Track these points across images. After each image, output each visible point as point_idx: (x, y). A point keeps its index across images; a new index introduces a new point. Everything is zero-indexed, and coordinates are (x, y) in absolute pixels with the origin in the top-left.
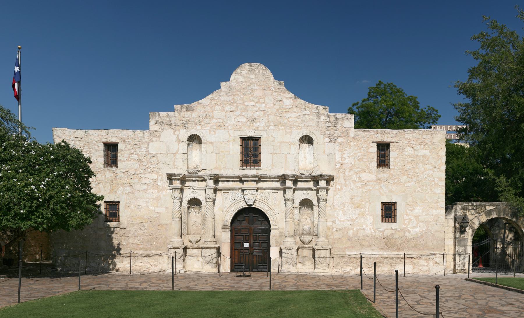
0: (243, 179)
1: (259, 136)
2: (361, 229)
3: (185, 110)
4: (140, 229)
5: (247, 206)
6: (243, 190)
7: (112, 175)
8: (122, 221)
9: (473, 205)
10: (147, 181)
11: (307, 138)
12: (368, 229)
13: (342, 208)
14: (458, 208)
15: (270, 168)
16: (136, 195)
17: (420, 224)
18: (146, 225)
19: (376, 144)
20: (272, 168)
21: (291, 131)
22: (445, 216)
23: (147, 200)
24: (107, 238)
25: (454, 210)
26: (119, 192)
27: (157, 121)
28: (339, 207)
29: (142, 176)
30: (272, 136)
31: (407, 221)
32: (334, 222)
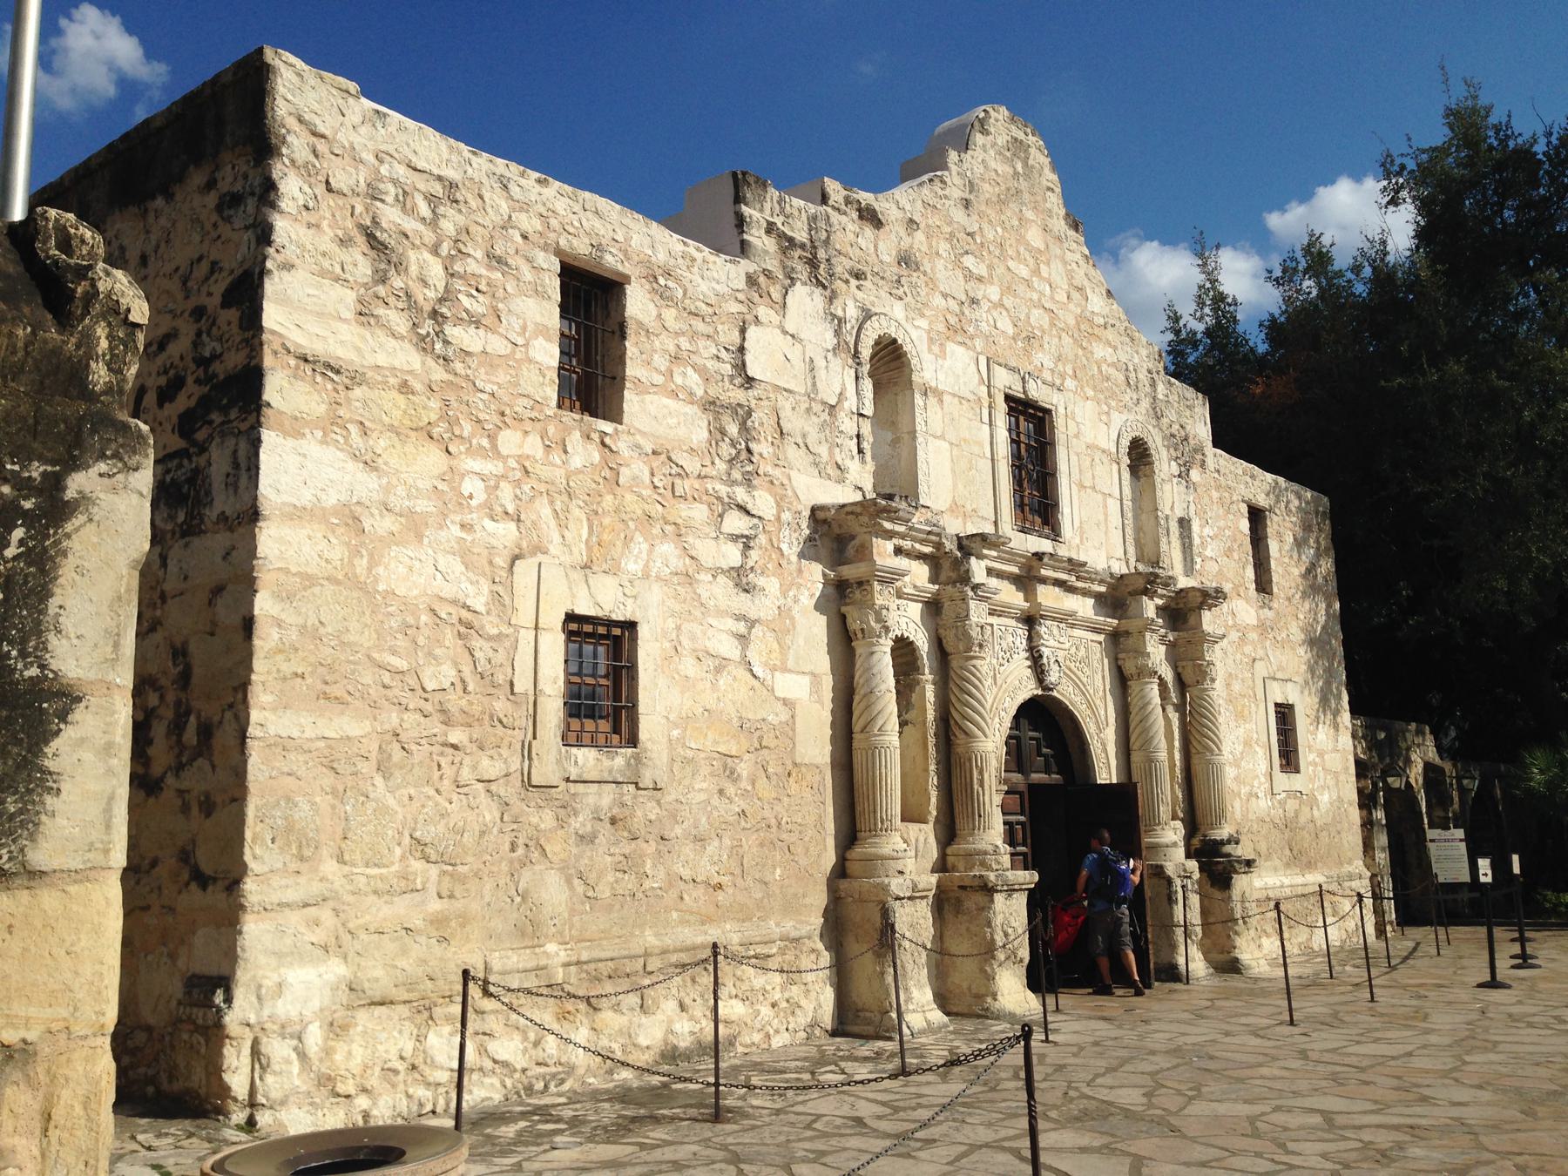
0: (1043, 572)
1: (1048, 406)
3: (855, 215)
4: (721, 792)
5: (1040, 692)
6: (1030, 621)
7: (596, 457)
8: (649, 745)
10: (736, 523)
16: (702, 590)
18: (744, 769)
19: (1244, 509)
23: (741, 627)
24: (574, 850)
26: (632, 566)
29: (723, 490)
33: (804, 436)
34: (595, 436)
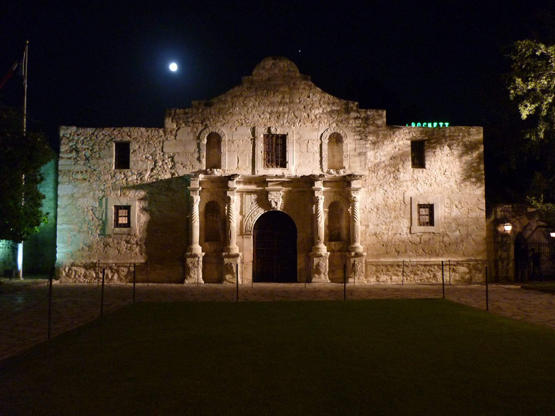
2: (396, 234)
7: (123, 176)
9: (513, 207)
11: (335, 135)
12: (404, 233)
13: (375, 210)
14: (498, 210)
15: (297, 168)
17: (460, 228)
20: (298, 168)
21: (319, 128)
22: (485, 219)
25: (493, 213)
27: (172, 119)
28: (372, 210)
30: (298, 133)
31: (445, 224)
32: (367, 226)
33: (181, 161)
34: (123, 173)
